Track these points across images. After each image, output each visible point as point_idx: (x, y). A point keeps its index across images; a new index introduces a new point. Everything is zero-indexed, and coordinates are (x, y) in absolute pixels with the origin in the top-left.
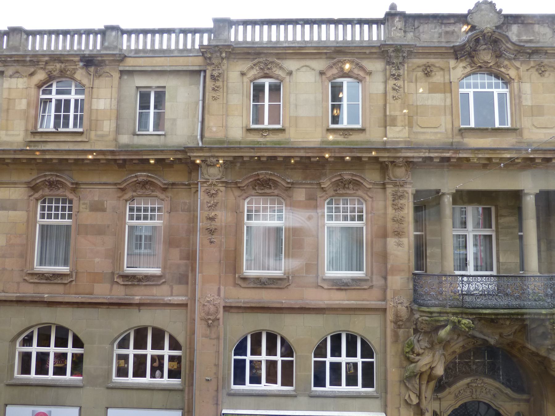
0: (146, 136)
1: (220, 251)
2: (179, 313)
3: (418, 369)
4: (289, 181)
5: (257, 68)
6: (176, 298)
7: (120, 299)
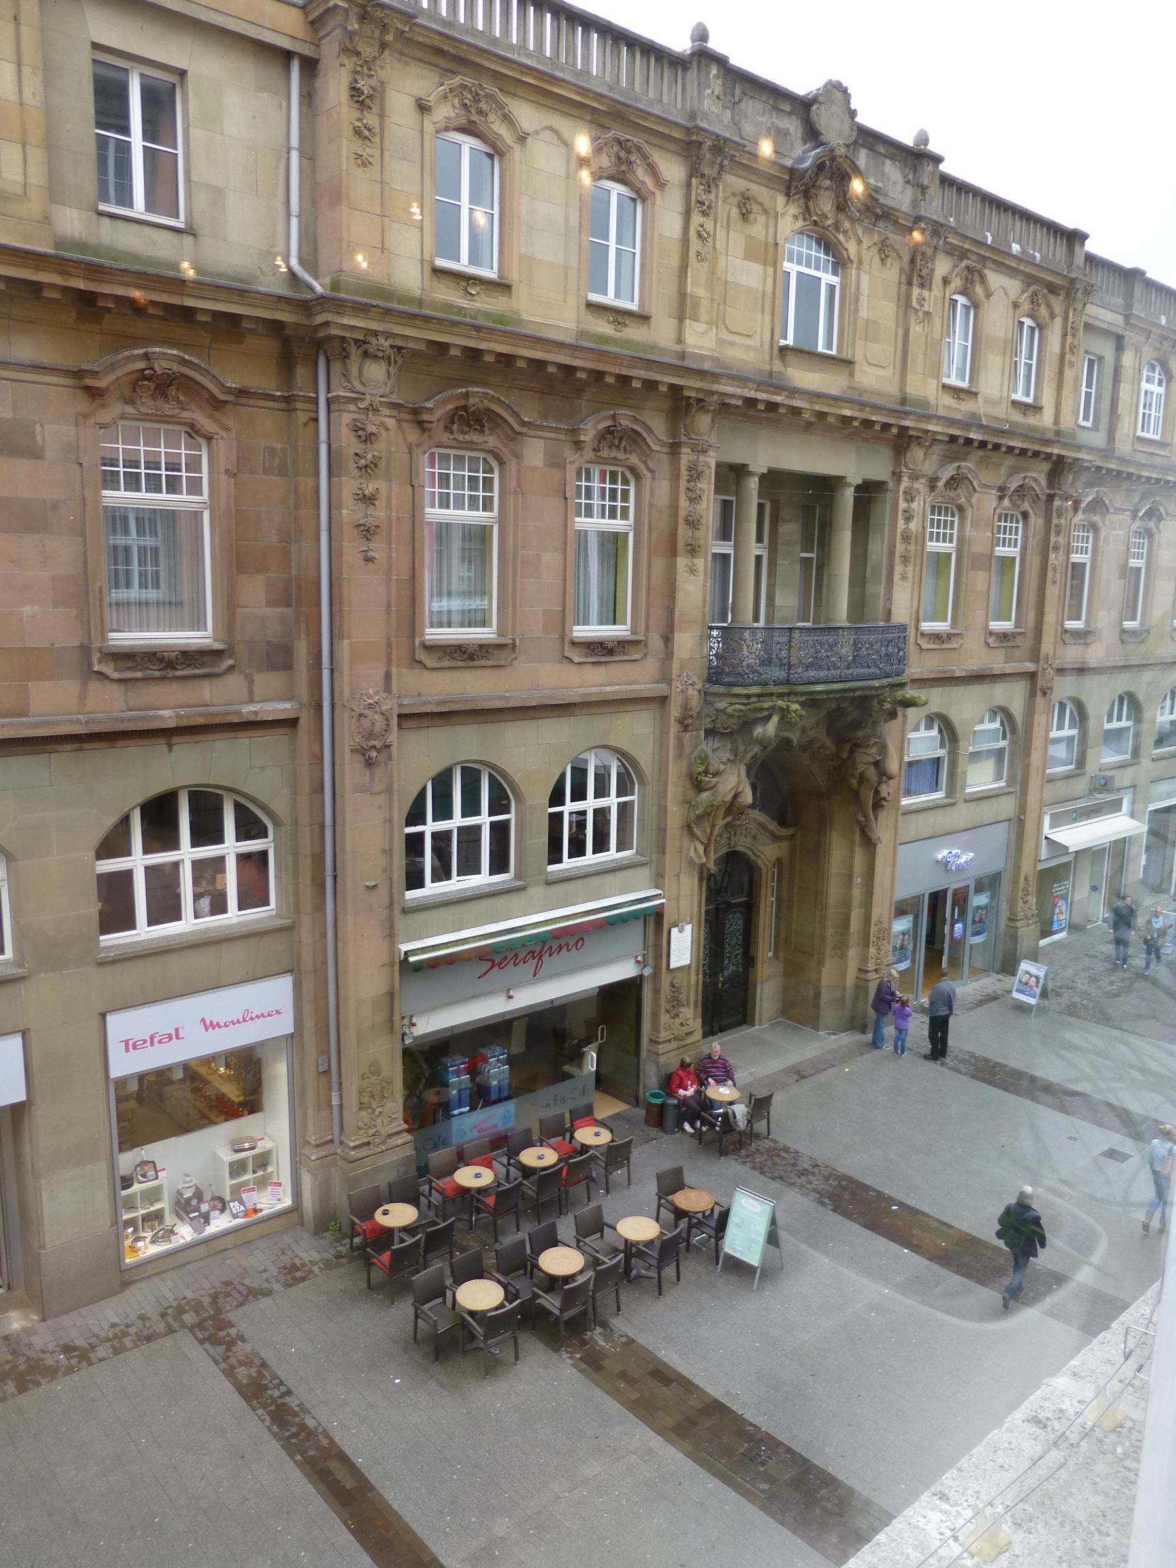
0: (137, 227)
1: (388, 581)
2: (271, 744)
3: (719, 799)
4: (526, 419)
5: (456, 100)
6: (267, 706)
7: (122, 721)
